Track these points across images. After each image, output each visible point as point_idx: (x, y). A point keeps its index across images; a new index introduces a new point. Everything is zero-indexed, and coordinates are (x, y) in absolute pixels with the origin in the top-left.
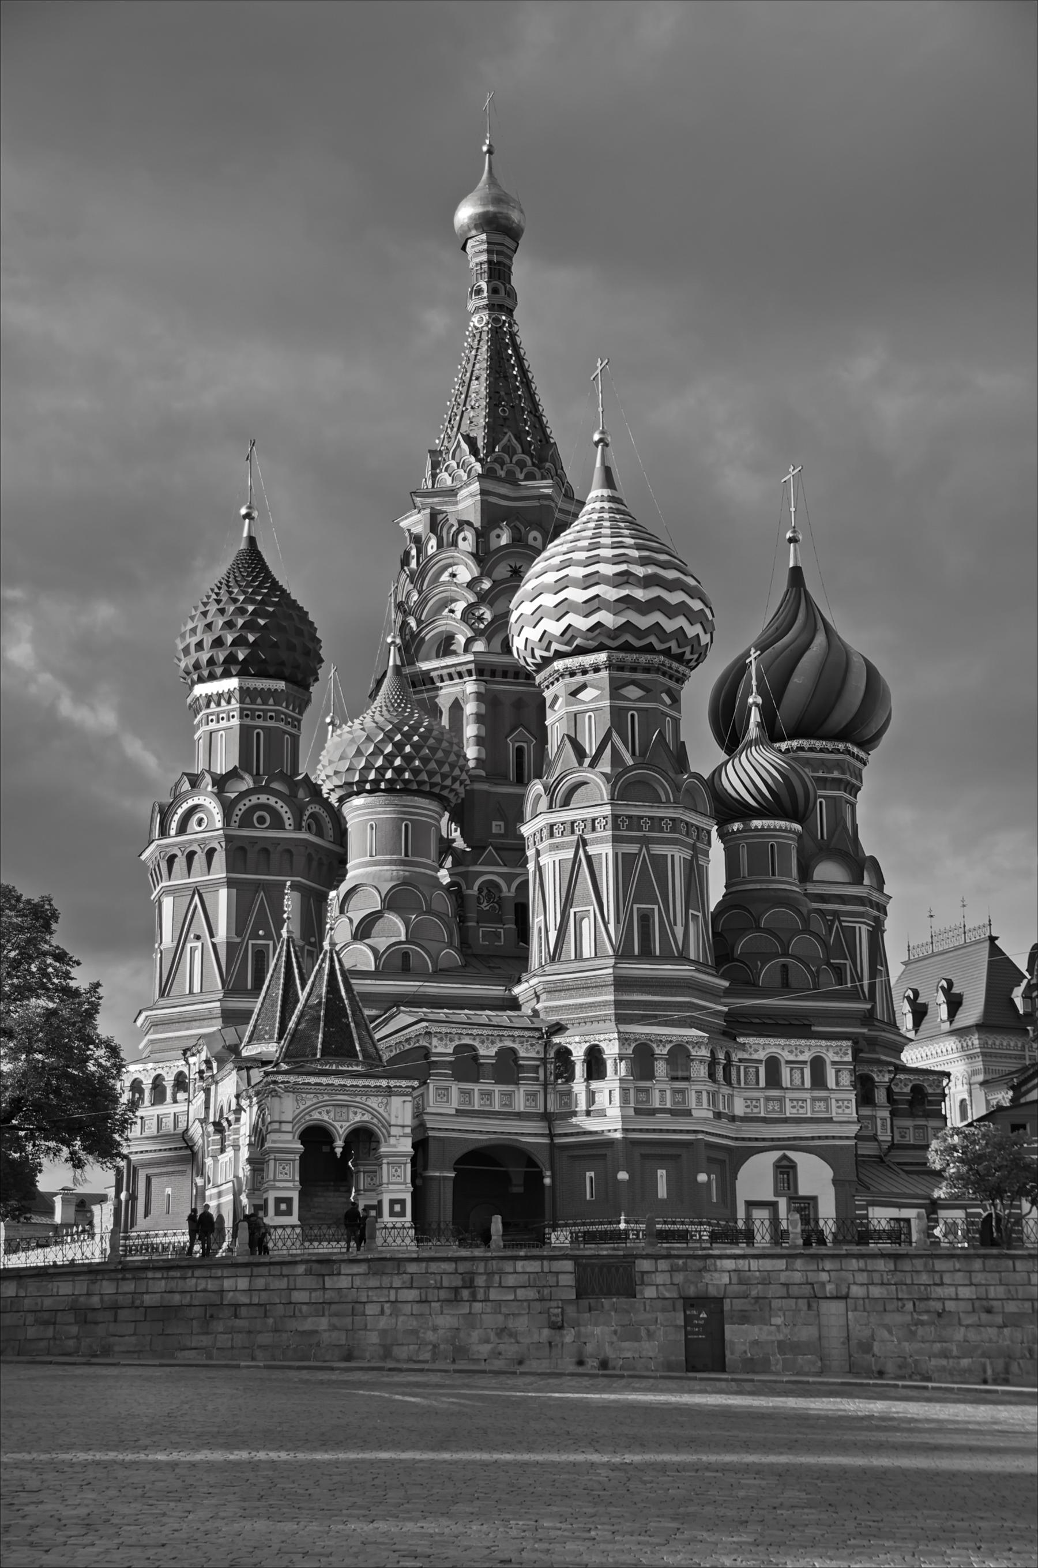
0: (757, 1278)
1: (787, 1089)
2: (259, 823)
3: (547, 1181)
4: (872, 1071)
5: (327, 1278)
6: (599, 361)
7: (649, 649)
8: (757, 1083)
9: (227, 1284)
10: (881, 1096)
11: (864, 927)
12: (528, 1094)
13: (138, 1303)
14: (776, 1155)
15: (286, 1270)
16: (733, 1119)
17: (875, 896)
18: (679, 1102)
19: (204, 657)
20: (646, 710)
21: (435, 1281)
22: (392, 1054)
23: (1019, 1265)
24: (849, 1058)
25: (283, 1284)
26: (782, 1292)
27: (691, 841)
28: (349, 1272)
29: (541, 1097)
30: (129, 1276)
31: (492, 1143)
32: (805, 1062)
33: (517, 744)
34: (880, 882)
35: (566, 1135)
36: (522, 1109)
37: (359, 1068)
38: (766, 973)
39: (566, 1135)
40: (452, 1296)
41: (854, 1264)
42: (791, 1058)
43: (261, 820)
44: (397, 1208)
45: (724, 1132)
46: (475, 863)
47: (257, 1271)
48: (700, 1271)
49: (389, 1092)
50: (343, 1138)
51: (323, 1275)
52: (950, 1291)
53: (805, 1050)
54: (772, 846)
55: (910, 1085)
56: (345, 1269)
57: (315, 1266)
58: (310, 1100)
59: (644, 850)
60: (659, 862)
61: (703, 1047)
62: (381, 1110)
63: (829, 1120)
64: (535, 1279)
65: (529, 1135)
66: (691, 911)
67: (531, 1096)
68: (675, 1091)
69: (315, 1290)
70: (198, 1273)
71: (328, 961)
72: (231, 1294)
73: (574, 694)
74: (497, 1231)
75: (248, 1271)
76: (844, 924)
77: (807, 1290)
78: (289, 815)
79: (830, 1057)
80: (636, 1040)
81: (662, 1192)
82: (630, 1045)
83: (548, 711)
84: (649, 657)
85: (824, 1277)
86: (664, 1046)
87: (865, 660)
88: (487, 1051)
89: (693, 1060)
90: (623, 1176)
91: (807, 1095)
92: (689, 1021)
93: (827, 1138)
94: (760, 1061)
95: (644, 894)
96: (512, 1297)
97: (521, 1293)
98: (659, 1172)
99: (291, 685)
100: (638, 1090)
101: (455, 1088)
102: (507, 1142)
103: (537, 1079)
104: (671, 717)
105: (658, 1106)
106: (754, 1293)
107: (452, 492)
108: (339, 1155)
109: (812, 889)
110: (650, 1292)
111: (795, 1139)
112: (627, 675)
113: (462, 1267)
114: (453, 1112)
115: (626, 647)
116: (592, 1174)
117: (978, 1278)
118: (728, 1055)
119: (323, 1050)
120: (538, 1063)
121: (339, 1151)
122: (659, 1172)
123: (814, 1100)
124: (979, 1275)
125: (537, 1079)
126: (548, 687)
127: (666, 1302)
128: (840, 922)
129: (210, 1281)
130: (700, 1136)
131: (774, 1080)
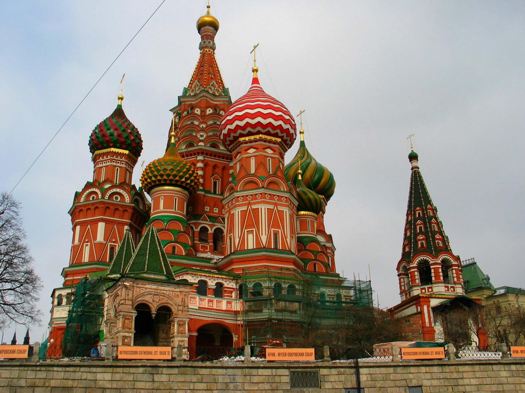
0: (379, 377)
5: (155, 376)
7: (276, 135)
9: (99, 376)
13: (47, 384)
20: (274, 158)
25: (131, 378)
26: (392, 384)
30: (43, 369)
40: (224, 387)
41: (423, 369)
42: (329, 293)
46: (199, 220)
47: (115, 369)
52: (466, 381)
56: (165, 371)
57: (148, 369)
59: (275, 208)
60: (281, 213)
70: (82, 369)
72: (101, 382)
75: (111, 370)
78: (128, 197)
84: (276, 138)
85: (411, 376)
86: (286, 284)
88: (212, 284)
96: (257, 388)
97: (261, 386)
99: (131, 153)
106: (378, 384)
110: (328, 386)
115: (268, 133)
117: (478, 375)
125: (232, 297)
129: (89, 374)
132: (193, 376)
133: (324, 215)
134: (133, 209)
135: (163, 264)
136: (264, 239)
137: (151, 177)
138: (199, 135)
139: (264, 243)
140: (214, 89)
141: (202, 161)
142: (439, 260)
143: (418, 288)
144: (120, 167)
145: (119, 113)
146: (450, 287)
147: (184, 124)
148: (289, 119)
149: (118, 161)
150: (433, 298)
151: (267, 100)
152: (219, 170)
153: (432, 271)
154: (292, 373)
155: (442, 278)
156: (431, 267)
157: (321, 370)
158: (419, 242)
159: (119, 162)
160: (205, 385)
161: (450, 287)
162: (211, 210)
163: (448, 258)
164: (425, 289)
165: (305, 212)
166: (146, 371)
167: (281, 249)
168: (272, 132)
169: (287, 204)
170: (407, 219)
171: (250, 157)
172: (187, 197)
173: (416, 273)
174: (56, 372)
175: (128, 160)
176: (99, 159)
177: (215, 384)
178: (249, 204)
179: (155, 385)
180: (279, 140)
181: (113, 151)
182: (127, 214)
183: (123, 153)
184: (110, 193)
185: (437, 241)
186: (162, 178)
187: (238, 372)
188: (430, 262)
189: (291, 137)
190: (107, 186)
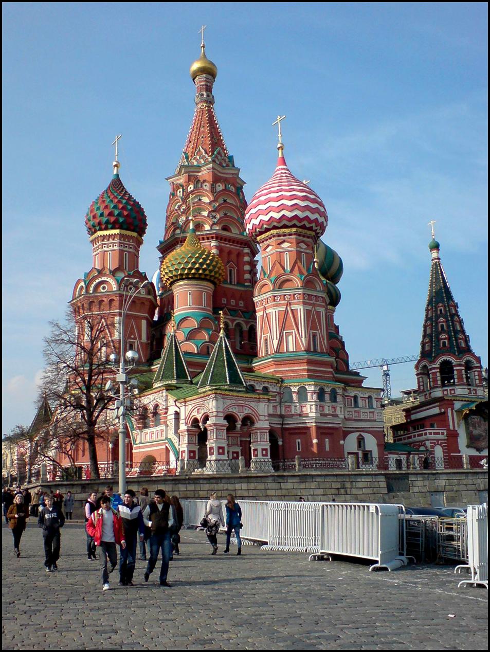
3: (280, 443)
5: (281, 484)
6: (279, 117)
7: (311, 229)
8: (351, 405)
14: (358, 434)
19: (104, 219)
29: (278, 408)
30: (191, 482)
33: (230, 268)
39: (288, 424)
44: (264, 452)
58: (229, 402)
60: (318, 313)
63: (375, 421)
64: (370, 485)
65: (274, 423)
67: (275, 407)
69: (277, 489)
71: (223, 342)
72: (240, 491)
73: (280, 244)
77: (473, 487)
84: (311, 232)
103: (276, 400)
106: (455, 489)
107: (199, 167)
110: (416, 489)
111: (363, 428)
112: (302, 238)
115: (303, 227)
116: (299, 440)
126: (263, 242)
127: (423, 494)
144: (128, 252)
145: (117, 184)
146: (472, 390)
148: (317, 208)
151: (302, 189)
152: (233, 257)
153: (455, 372)
156: (454, 368)
160: (322, 490)
161: (472, 390)
162: (228, 302)
164: (447, 390)
167: (319, 351)
168: (308, 225)
170: (427, 315)
177: (330, 490)
179: (283, 492)
180: (313, 233)
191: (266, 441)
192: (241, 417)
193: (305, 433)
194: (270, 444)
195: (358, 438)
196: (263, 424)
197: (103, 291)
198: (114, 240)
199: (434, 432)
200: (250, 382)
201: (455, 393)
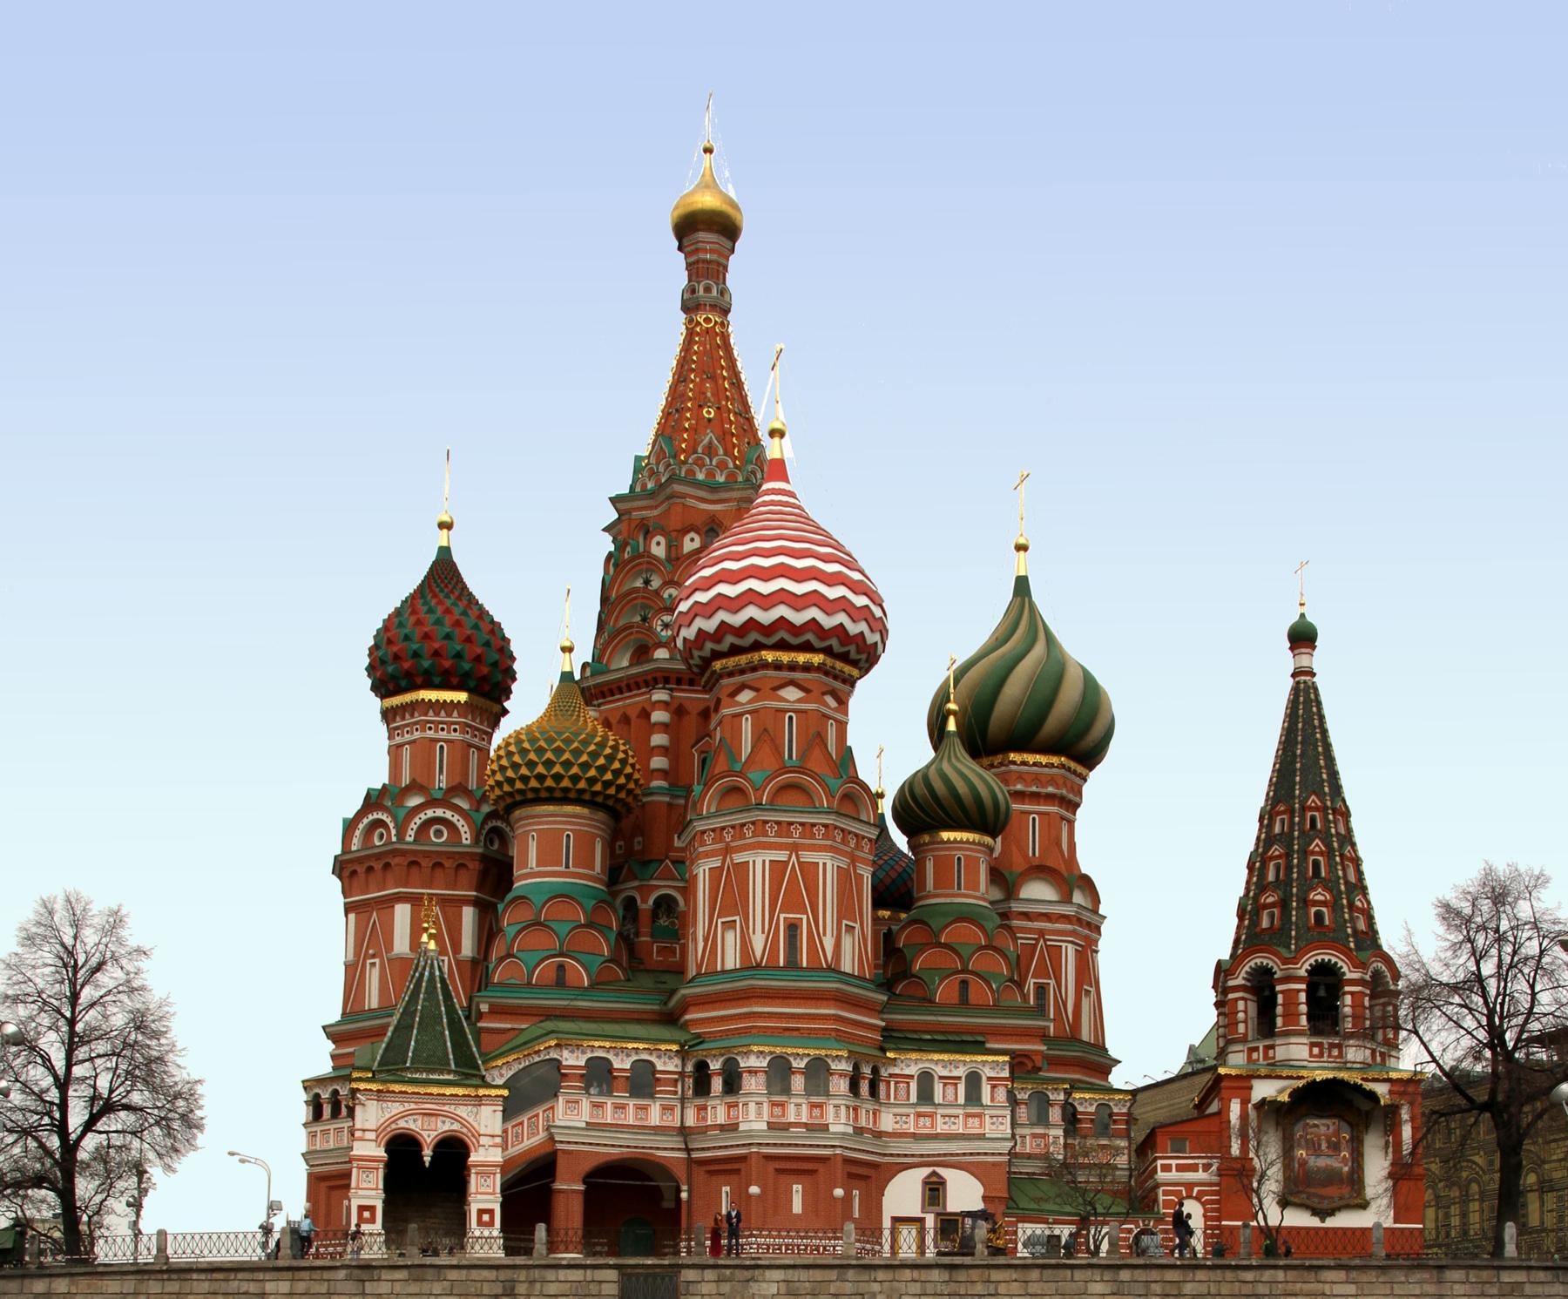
0: (806, 1289)
1: (939, 1105)
2: (436, 837)
4: (1047, 1089)
5: (367, 1284)
8: (908, 1099)
9: (269, 1287)
10: (1055, 1114)
11: (1070, 946)
12: (664, 1108)
14: (927, 1171)
15: (326, 1275)
16: (879, 1135)
17: (1086, 916)
18: (816, 1117)
21: (476, 1289)
22: (521, 1067)
23: (1078, 1274)
24: (1006, 1074)
25: (323, 1288)
27: (849, 850)
28: (389, 1278)
30: (174, 1276)
31: (625, 1156)
32: (959, 1078)
34: (1096, 899)
35: (703, 1149)
36: (658, 1124)
37: (451, 1077)
38: (943, 991)
41: (907, 1274)
42: (945, 1073)
43: (439, 833)
44: (486, 1217)
45: (864, 1150)
46: (651, 878)
48: (748, 1281)
49: (479, 1101)
50: (431, 1147)
51: (364, 1281)
53: (958, 1066)
54: (959, 859)
55: (1096, 1104)
56: (385, 1275)
57: (356, 1272)
58: (396, 1108)
59: (794, 856)
60: (810, 870)
61: (843, 1062)
62: (470, 1120)
64: (577, 1288)
65: (665, 1149)
66: (845, 922)
68: (813, 1106)
70: (240, 1275)
71: (427, 969)
74: (541, 1239)
75: (289, 1275)
76: (1049, 943)
79: (987, 1072)
80: (771, 1053)
81: (797, 1207)
82: (764, 1058)
83: (713, 715)
85: (876, 1287)
86: (802, 1059)
87: (1082, 667)
88: (622, 1063)
89: (832, 1074)
90: (754, 1190)
91: (960, 1112)
92: (833, 1034)
93: (979, 1154)
94: (911, 1077)
95: (793, 904)
98: (795, 1187)
100: (773, 1104)
101: (585, 1104)
102: (637, 1156)
103: (675, 1093)
104: (836, 720)
105: (793, 1120)
108: (427, 1165)
109: (1016, 907)
111: (945, 1155)
113: (503, 1275)
114: (584, 1125)
116: (728, 1188)
118: (875, 1071)
119: (413, 1058)
120: (676, 1076)
121: (427, 1159)
122: (795, 1187)
123: (967, 1116)
124: (1035, 1284)
125: (675, 1093)
128: (1045, 940)
129: (252, 1284)
130: (838, 1151)
131: (926, 1096)
132: (436, 1284)
133: (1079, 811)
134: (481, 861)
135: (449, 1044)
136: (758, 942)
137: (519, 766)
138: (659, 622)
139: (758, 954)
140: (711, 464)
141: (665, 705)
142: (1300, 968)
143: (1240, 1047)
144: (446, 741)
147: (626, 588)
149: (441, 726)
150: (1260, 1077)
154: (625, 1278)
155: (1304, 1020)
156: (1278, 988)
157: (684, 1272)
158: (1266, 912)
159: (445, 726)
163: (1334, 960)
164: (1256, 1049)
165: (950, 833)
166: (351, 1274)
169: (829, 843)
171: (741, 715)
172: (603, 826)
173: (1241, 1005)
174: (195, 1282)
175: (470, 717)
176: (394, 721)
178: (727, 851)
181: (423, 700)
182: (464, 876)
183: (452, 701)
184: (419, 822)
185: (1313, 910)
186: (526, 785)
187: (522, 1275)
188: (1275, 973)
189: (857, 646)
190: (414, 801)
191: (493, 1194)
192: (429, 1140)
193: (738, 1171)
194: (501, 1199)
195: (926, 1183)
196: (486, 1155)
197: (377, 843)
198: (412, 716)
199: (1177, 1165)
200: (592, 1051)
201: (1274, 1058)
